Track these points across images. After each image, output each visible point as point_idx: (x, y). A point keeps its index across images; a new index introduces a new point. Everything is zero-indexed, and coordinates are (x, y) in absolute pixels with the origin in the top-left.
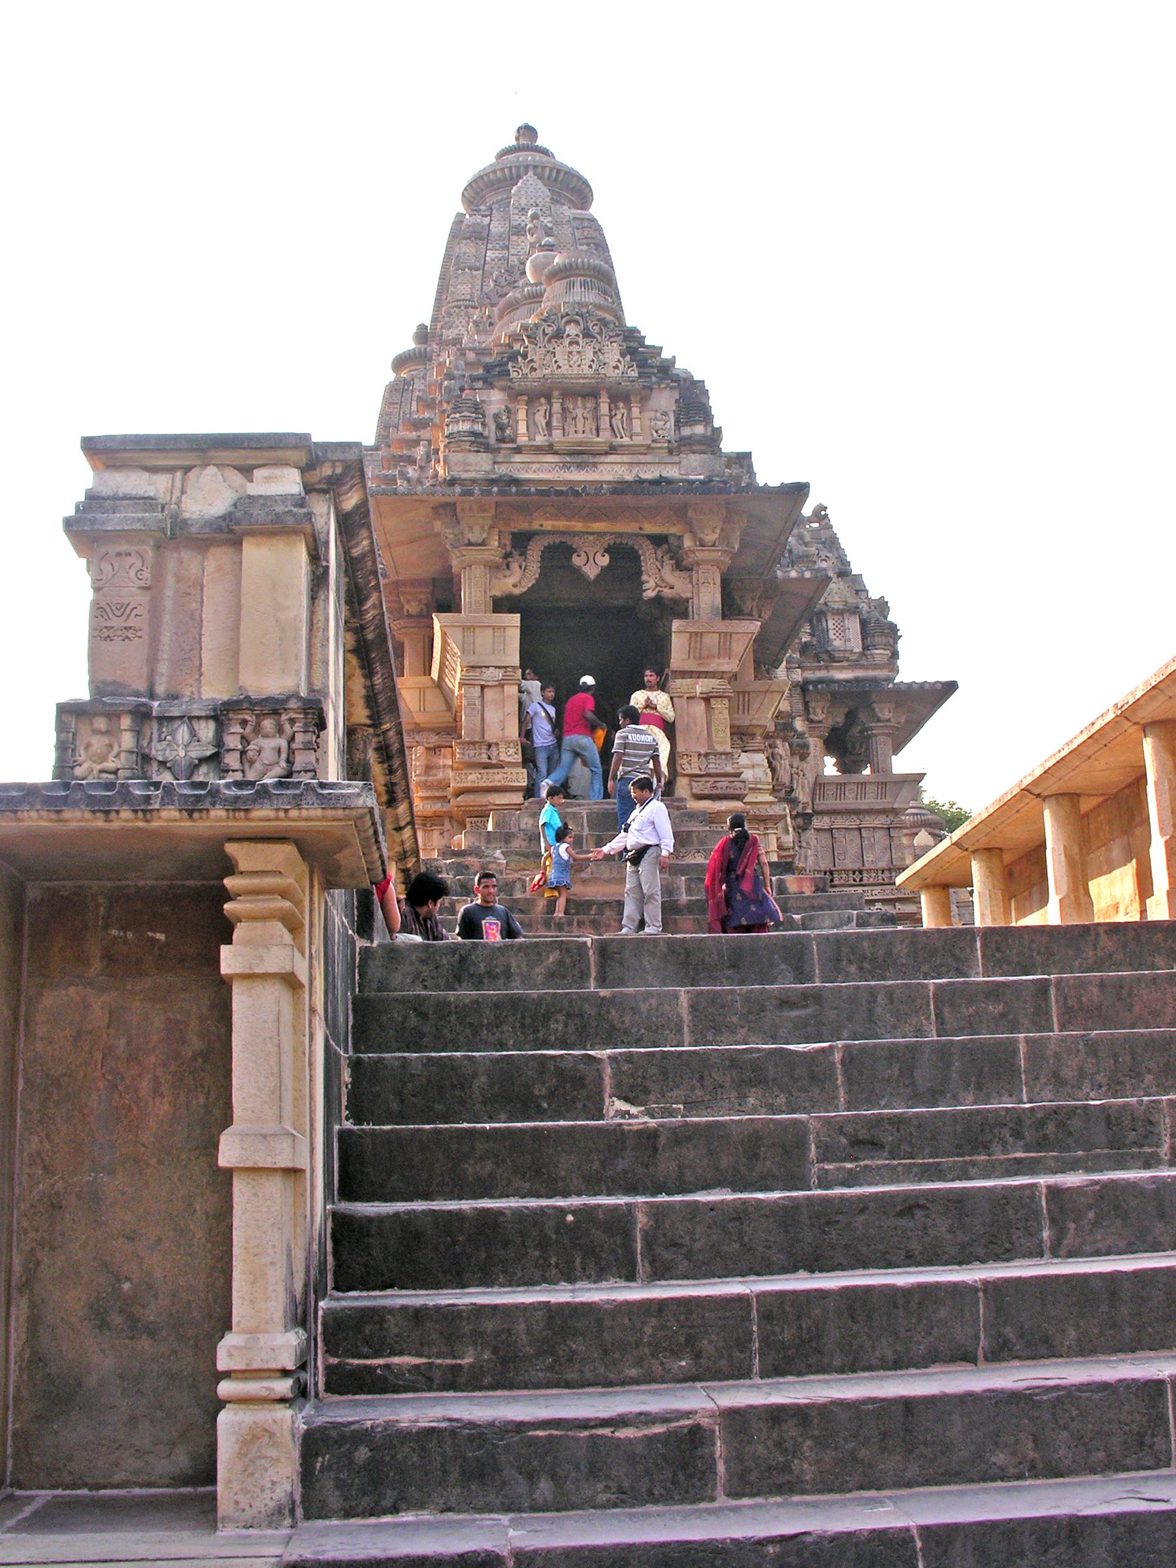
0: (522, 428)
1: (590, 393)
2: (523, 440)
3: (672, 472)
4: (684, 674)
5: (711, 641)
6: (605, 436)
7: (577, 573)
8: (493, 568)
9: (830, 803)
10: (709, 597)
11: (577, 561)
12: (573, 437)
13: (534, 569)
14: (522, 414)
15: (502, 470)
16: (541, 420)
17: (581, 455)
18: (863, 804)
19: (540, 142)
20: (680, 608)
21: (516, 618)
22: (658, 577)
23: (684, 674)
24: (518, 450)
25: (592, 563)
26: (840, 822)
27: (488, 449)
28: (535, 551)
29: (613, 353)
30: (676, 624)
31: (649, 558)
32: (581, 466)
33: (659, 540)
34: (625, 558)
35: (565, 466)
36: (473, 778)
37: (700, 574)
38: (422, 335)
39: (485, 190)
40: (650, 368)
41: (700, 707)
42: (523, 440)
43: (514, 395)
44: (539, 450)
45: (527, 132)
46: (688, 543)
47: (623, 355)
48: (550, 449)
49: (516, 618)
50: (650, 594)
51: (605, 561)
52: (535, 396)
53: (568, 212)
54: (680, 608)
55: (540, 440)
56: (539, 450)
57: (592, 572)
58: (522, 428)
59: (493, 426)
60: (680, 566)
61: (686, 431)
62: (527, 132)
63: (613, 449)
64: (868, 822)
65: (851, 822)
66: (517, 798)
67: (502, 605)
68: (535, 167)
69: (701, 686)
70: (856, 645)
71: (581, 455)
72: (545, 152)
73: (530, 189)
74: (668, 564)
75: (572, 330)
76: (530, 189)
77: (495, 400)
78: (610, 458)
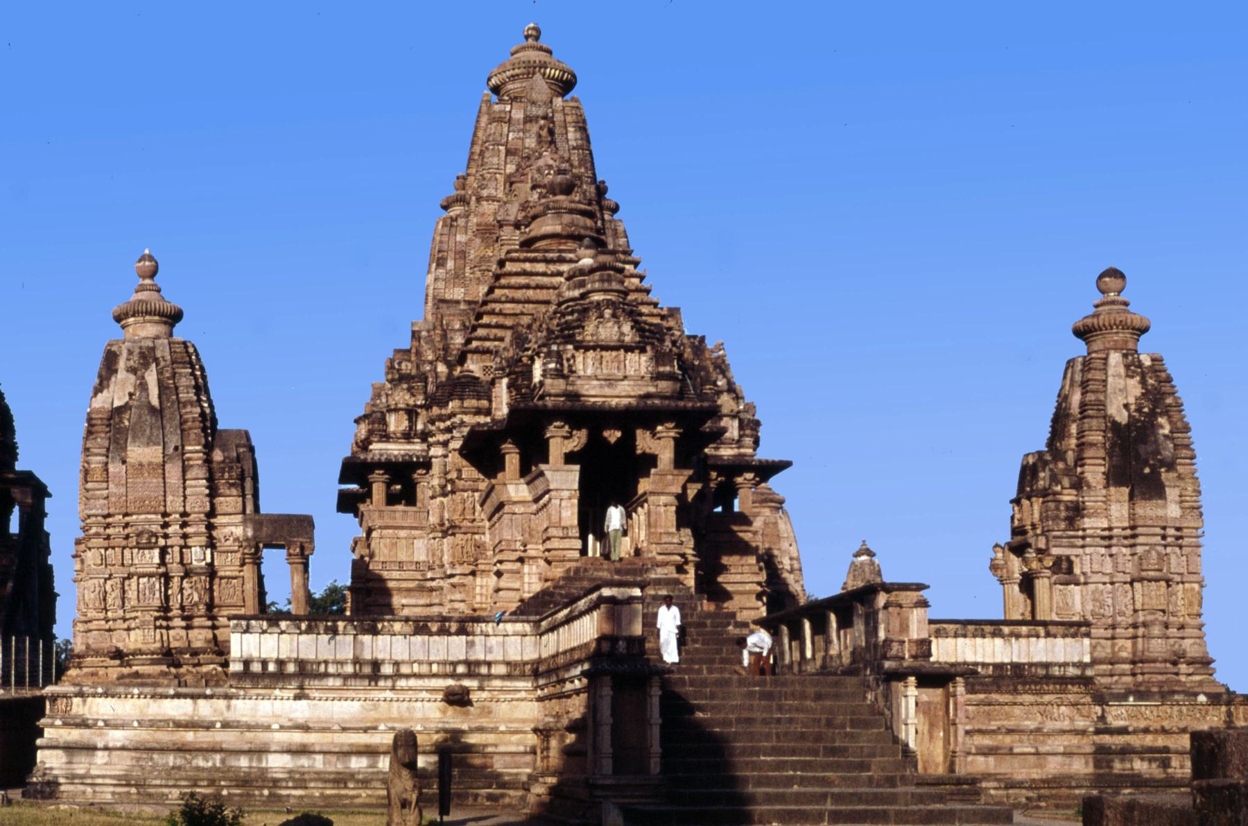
2: (581, 373)
13: (584, 440)
16: (590, 362)
17: (610, 381)
19: (543, 42)
21: (577, 467)
25: (613, 435)
44: (589, 378)
47: (632, 328)
49: (577, 467)
50: (639, 452)
55: (589, 372)
57: (613, 440)
61: (661, 369)
63: (625, 377)
67: (570, 458)
71: (610, 381)
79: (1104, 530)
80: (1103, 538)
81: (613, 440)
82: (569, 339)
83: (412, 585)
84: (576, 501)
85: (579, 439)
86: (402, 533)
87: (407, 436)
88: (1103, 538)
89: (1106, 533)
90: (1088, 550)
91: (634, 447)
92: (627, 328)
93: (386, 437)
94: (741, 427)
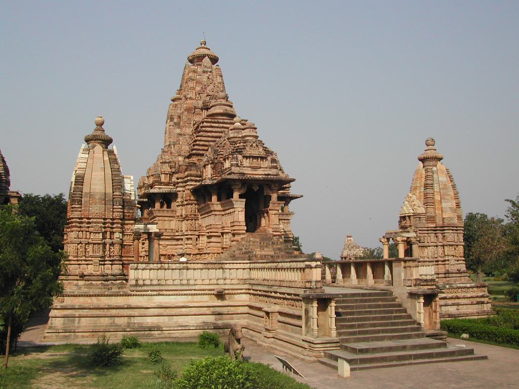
3: (270, 173)
7: (253, 190)
8: (240, 189)
11: (253, 188)
15: (241, 171)
21: (245, 200)
25: (256, 188)
27: (239, 166)
28: (246, 186)
29: (261, 149)
31: (265, 188)
33: (267, 185)
40: (268, 152)
43: (244, 157)
46: (273, 186)
50: (265, 194)
51: (258, 188)
52: (247, 157)
57: (256, 190)
58: (245, 163)
59: (239, 162)
66: (245, 232)
67: (241, 196)
68: (208, 55)
69: (274, 212)
74: (269, 189)
77: (240, 157)
78: (260, 169)
79: (434, 227)
80: (434, 230)
82: (240, 153)
83: (169, 237)
87: (168, 184)
88: (434, 230)
90: (429, 235)
93: (161, 183)
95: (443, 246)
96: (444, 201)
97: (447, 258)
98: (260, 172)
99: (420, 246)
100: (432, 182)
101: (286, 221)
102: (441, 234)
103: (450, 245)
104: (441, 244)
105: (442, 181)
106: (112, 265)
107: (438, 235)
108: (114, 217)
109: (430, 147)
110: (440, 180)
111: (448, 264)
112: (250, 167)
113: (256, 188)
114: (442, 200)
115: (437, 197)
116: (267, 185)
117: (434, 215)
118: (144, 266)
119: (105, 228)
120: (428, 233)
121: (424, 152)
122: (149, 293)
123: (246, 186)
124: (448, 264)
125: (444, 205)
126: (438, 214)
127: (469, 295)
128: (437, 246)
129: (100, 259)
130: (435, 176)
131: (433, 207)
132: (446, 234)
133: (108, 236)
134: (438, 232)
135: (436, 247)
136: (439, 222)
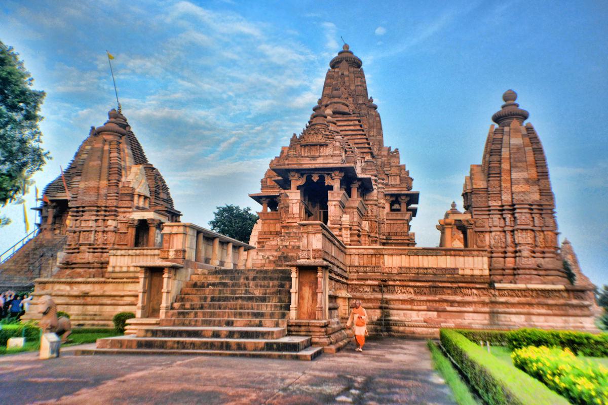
0: (303, 153)
1: (316, 145)
2: (303, 155)
3: (331, 161)
4: (331, 201)
5: (336, 195)
6: (318, 154)
9: (390, 218)
10: (336, 185)
11: (312, 178)
12: (312, 154)
14: (303, 150)
16: (306, 151)
18: (398, 218)
19: (350, 49)
20: (331, 188)
21: (299, 191)
22: (328, 182)
23: (331, 201)
24: (302, 157)
25: (315, 178)
26: (392, 222)
28: (305, 176)
30: (329, 192)
32: (314, 160)
34: (322, 178)
35: (311, 160)
36: (290, 220)
37: (335, 181)
38: (320, 101)
39: (335, 64)
41: (333, 207)
42: (303, 155)
43: (301, 146)
45: (346, 46)
46: (333, 175)
48: (308, 157)
51: (318, 178)
53: (352, 69)
54: (331, 188)
55: (306, 155)
56: (306, 157)
57: (315, 181)
58: (303, 153)
60: (332, 179)
62: (346, 46)
63: (320, 156)
64: (399, 222)
65: (395, 222)
67: (298, 188)
69: (334, 203)
70: (398, 182)
71: (314, 158)
72: (351, 53)
73: (344, 64)
74: (330, 178)
75: (312, 132)
76: (344, 64)
80: (499, 210)
81: (315, 181)
84: (298, 204)
85: (301, 182)
86: (272, 221)
88: (499, 210)
89: (501, 208)
90: (491, 216)
91: (324, 183)
92: (320, 136)
94: (401, 180)
95: (512, 231)
96: (515, 170)
97: (518, 248)
98: (320, 160)
99: (476, 232)
100: (499, 146)
101: (401, 222)
102: (509, 216)
103: (522, 230)
104: (511, 229)
105: (513, 145)
106: (102, 252)
107: (504, 216)
108: (107, 205)
109: (510, 102)
110: (511, 142)
111: (519, 256)
112: (308, 157)
113: (315, 178)
114: (512, 169)
115: (505, 166)
116: (328, 174)
117: (499, 189)
118: (123, 252)
119: (97, 216)
120: (489, 215)
121: (500, 109)
122: (125, 280)
123: (305, 176)
124: (519, 256)
125: (514, 175)
126: (505, 188)
127: (550, 302)
128: (505, 232)
129: (88, 247)
130: (505, 138)
131: (499, 179)
132: (516, 215)
133: (100, 223)
134: (504, 212)
135: (503, 234)
136: (506, 197)
